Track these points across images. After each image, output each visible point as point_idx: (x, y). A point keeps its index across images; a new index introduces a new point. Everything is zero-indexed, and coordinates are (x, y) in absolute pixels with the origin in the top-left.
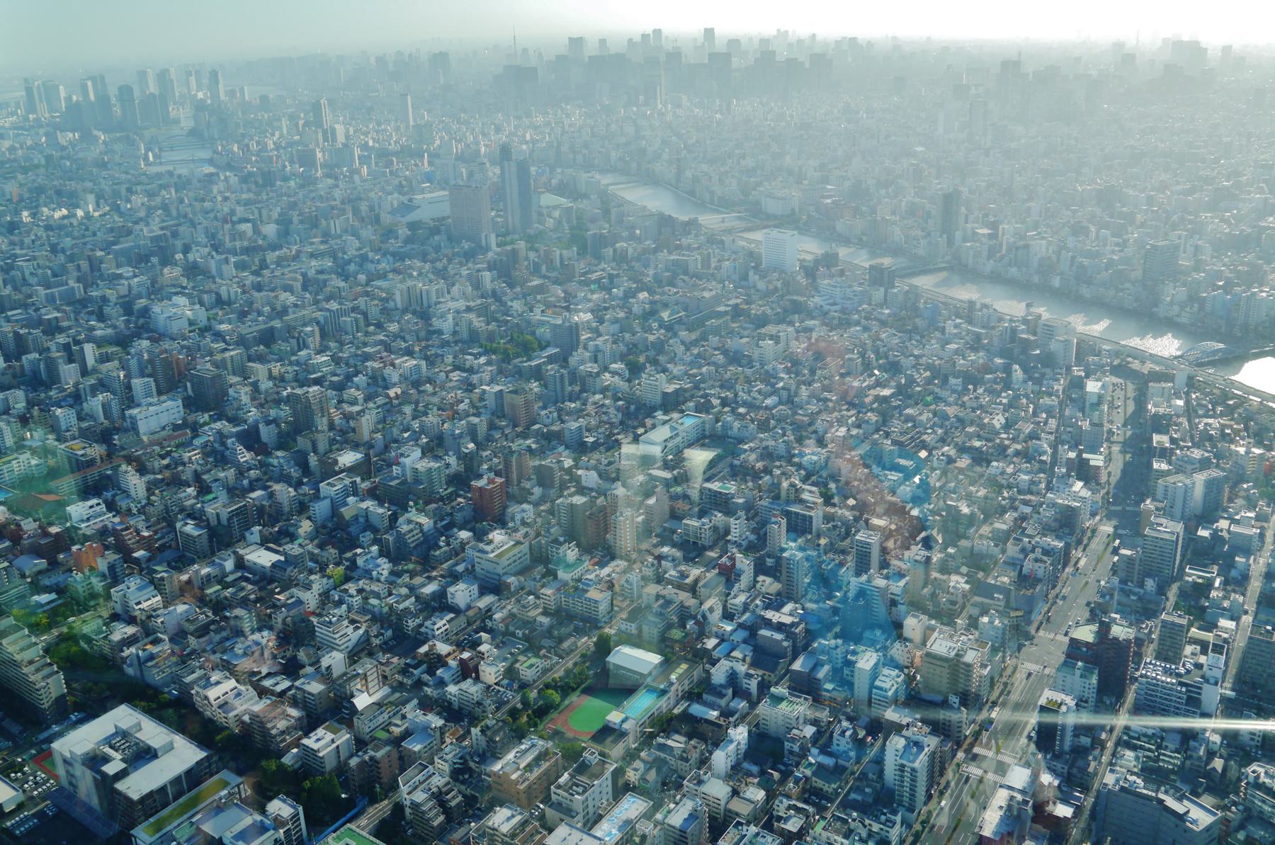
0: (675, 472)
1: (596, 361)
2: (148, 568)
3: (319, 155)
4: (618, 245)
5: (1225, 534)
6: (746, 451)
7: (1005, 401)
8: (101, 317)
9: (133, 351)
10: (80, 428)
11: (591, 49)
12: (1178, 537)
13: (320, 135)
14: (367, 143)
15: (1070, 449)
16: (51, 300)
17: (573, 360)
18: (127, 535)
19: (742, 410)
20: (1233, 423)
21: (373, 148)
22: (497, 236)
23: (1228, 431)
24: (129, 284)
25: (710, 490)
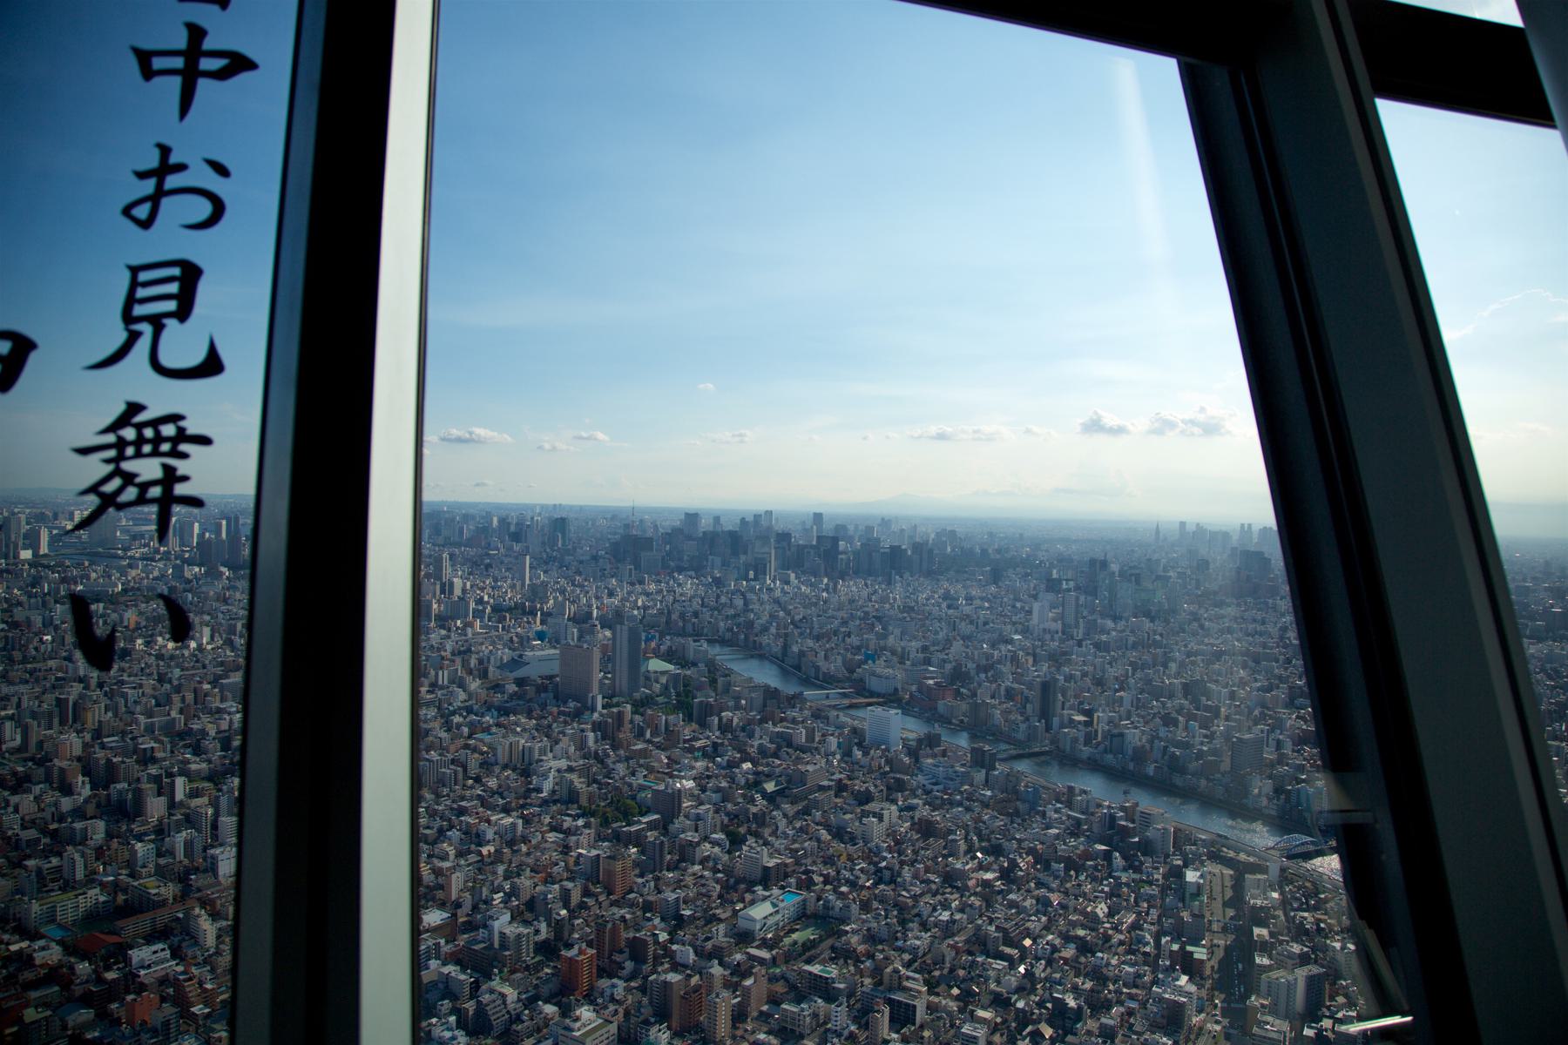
0: (774, 952)
1: (696, 831)
2: (205, 1025)
3: (435, 606)
4: (723, 714)
5: (1330, 1034)
6: (847, 932)
7: (1106, 889)
8: (198, 751)
9: (225, 787)
10: (157, 865)
11: (705, 524)
12: (1285, 1037)
13: (438, 587)
14: (482, 598)
15: (1172, 941)
16: (150, 729)
17: (672, 828)
18: (189, 986)
19: (844, 889)
20: (1326, 917)
21: (488, 603)
22: (604, 698)
23: (1322, 925)
24: (231, 720)
25: (810, 973)
